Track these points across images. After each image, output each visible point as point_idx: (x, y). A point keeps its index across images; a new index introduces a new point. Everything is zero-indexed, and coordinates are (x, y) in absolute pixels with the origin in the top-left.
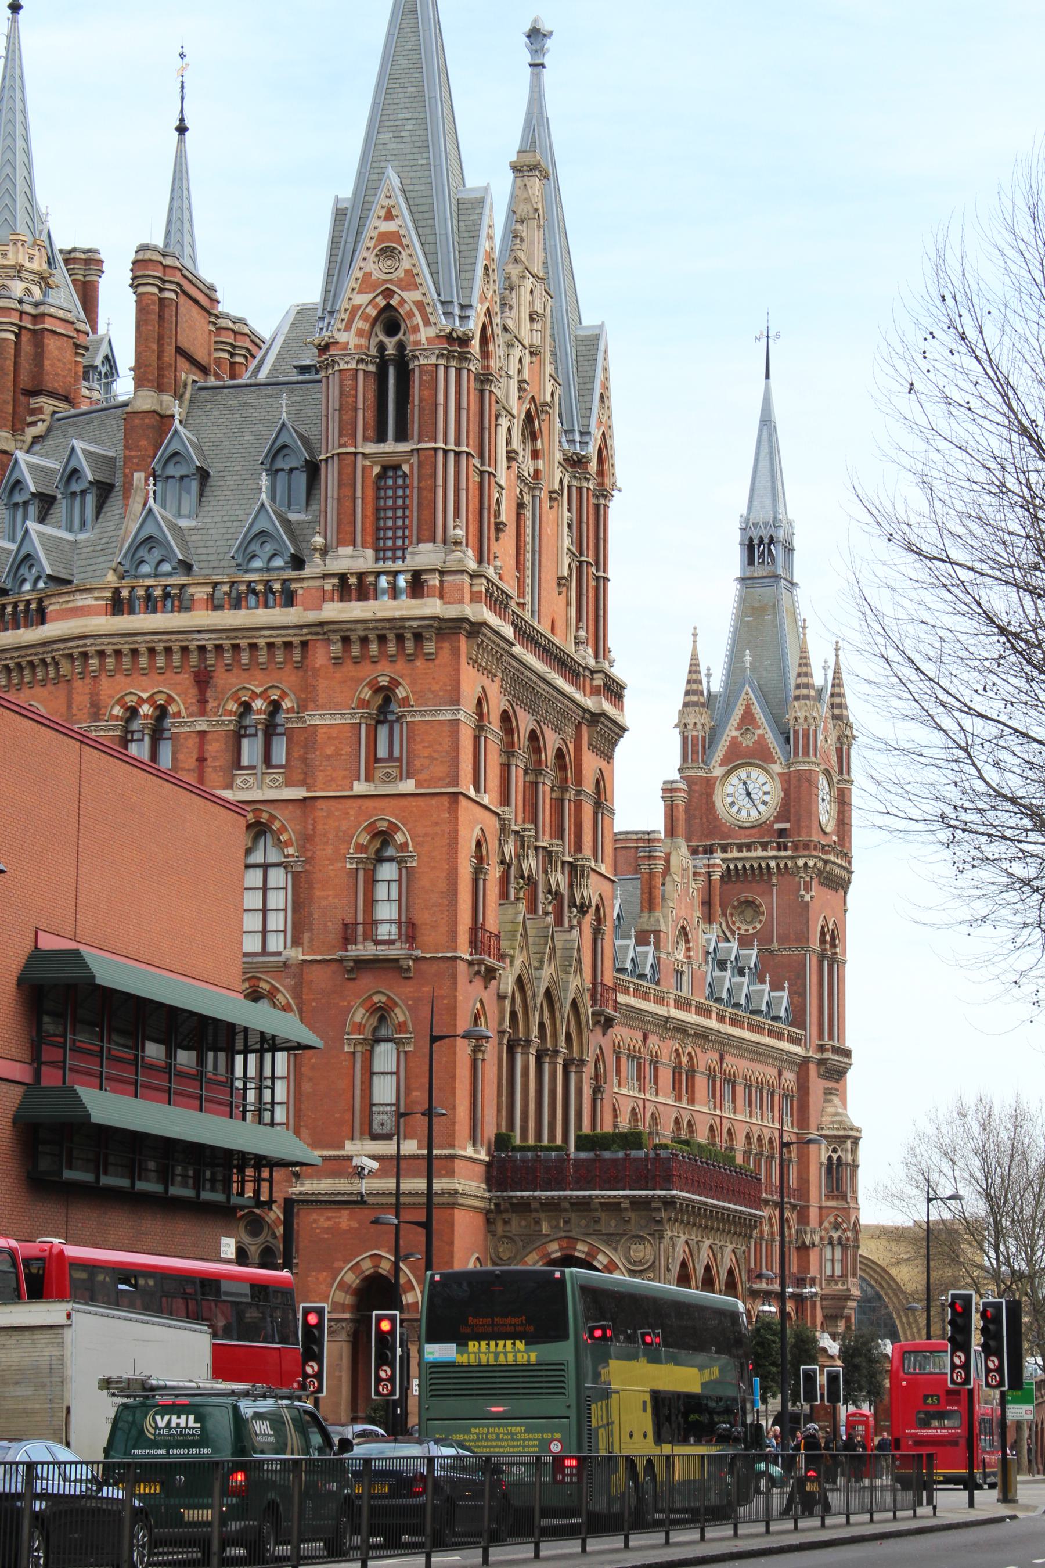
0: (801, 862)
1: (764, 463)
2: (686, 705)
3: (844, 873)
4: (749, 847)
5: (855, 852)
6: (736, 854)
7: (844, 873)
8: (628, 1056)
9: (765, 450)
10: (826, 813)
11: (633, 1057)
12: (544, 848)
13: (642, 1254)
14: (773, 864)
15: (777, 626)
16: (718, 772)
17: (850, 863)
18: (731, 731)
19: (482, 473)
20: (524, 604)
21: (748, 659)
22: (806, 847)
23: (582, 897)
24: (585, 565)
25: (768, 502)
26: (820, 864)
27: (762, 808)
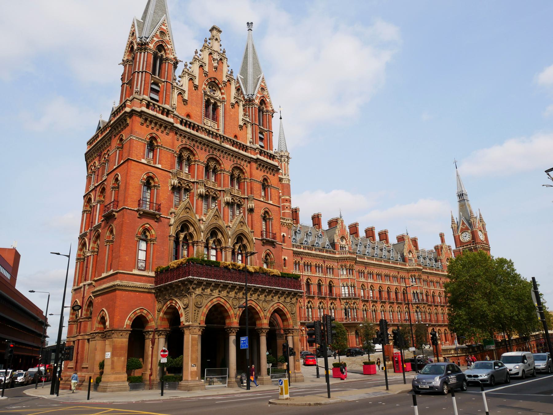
0: (477, 246)
1: (459, 182)
2: (452, 224)
3: (488, 248)
4: (467, 245)
5: (490, 244)
6: (465, 247)
7: (488, 248)
8: (436, 282)
9: (458, 180)
10: (482, 237)
11: (438, 283)
12: (223, 191)
13: (186, 302)
14: (472, 247)
15: (466, 207)
16: (460, 234)
17: (489, 245)
18: (461, 227)
19: (164, 82)
20: (219, 129)
21: (461, 214)
22: (478, 243)
23: (250, 206)
24: (254, 125)
25: (460, 188)
26: (481, 246)
27: (469, 238)
